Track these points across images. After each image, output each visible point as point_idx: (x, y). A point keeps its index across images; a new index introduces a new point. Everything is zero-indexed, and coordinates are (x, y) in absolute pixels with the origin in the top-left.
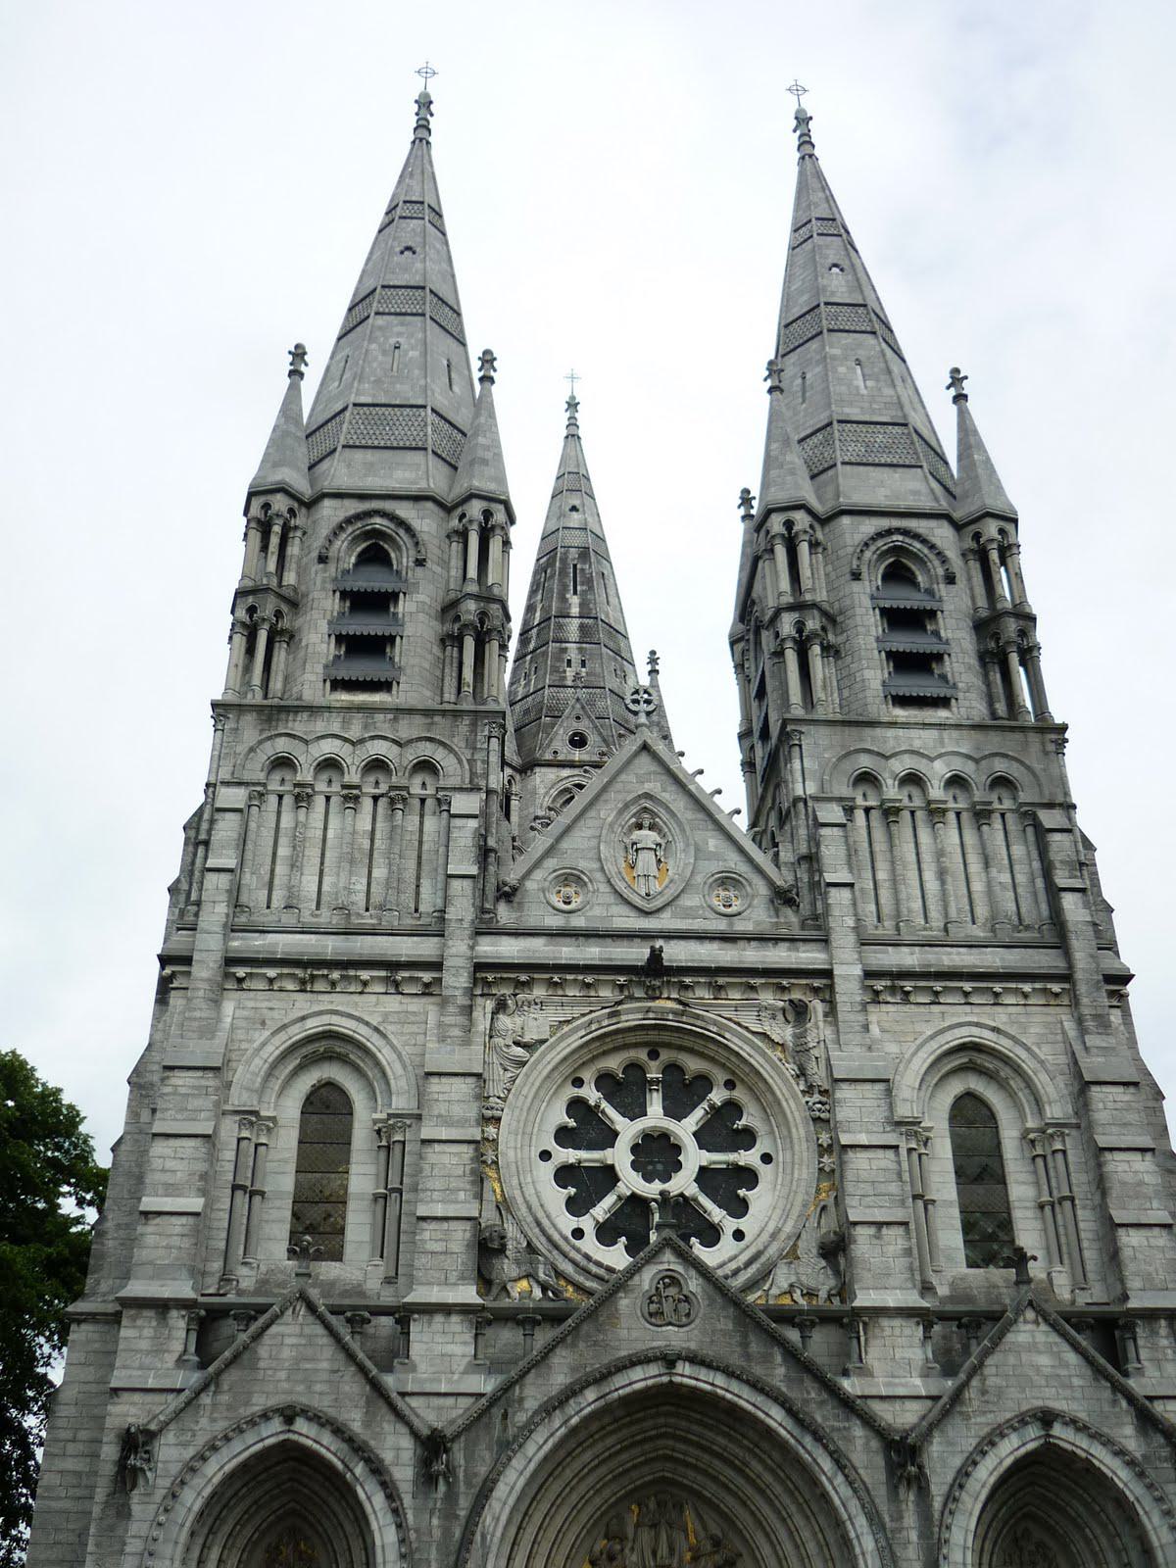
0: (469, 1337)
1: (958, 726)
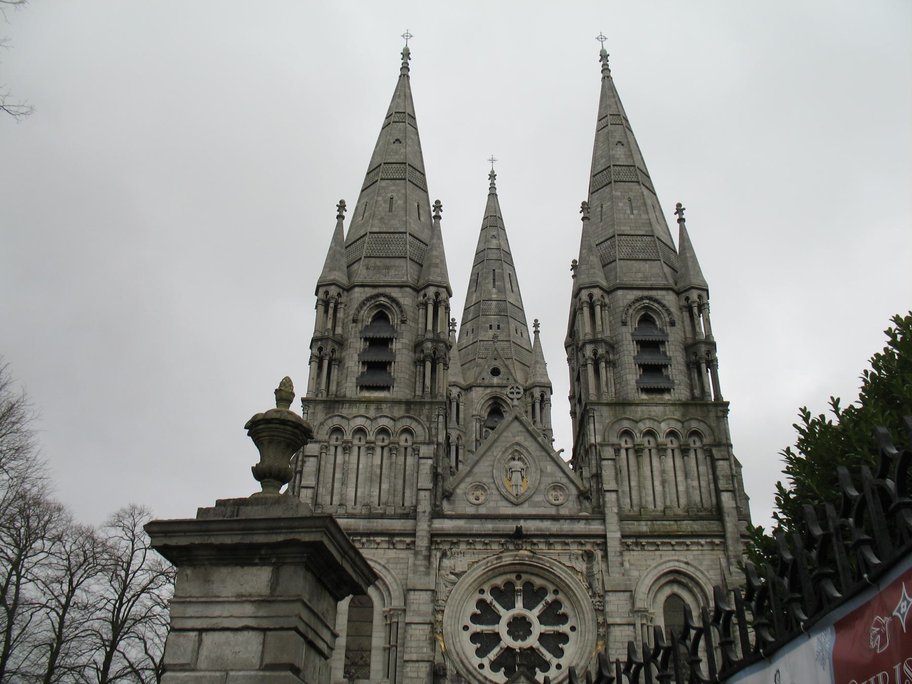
1: (673, 404)
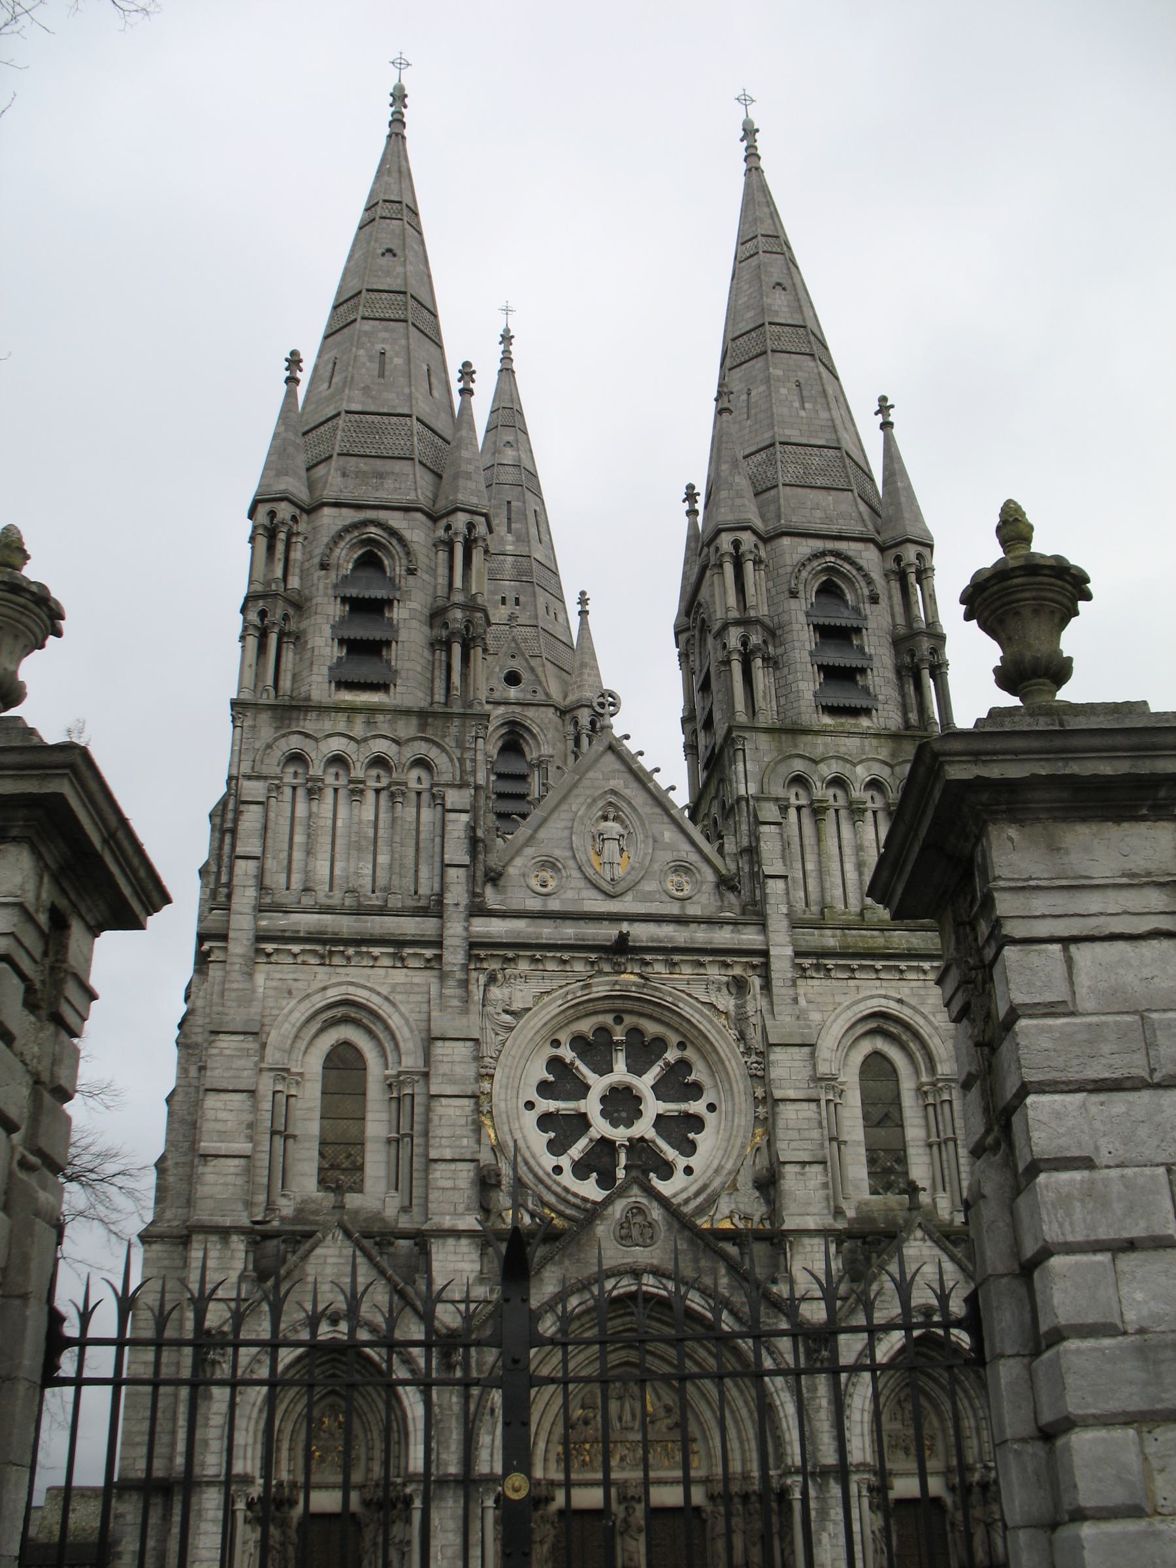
0: (475, 1256)
1: (877, 735)
